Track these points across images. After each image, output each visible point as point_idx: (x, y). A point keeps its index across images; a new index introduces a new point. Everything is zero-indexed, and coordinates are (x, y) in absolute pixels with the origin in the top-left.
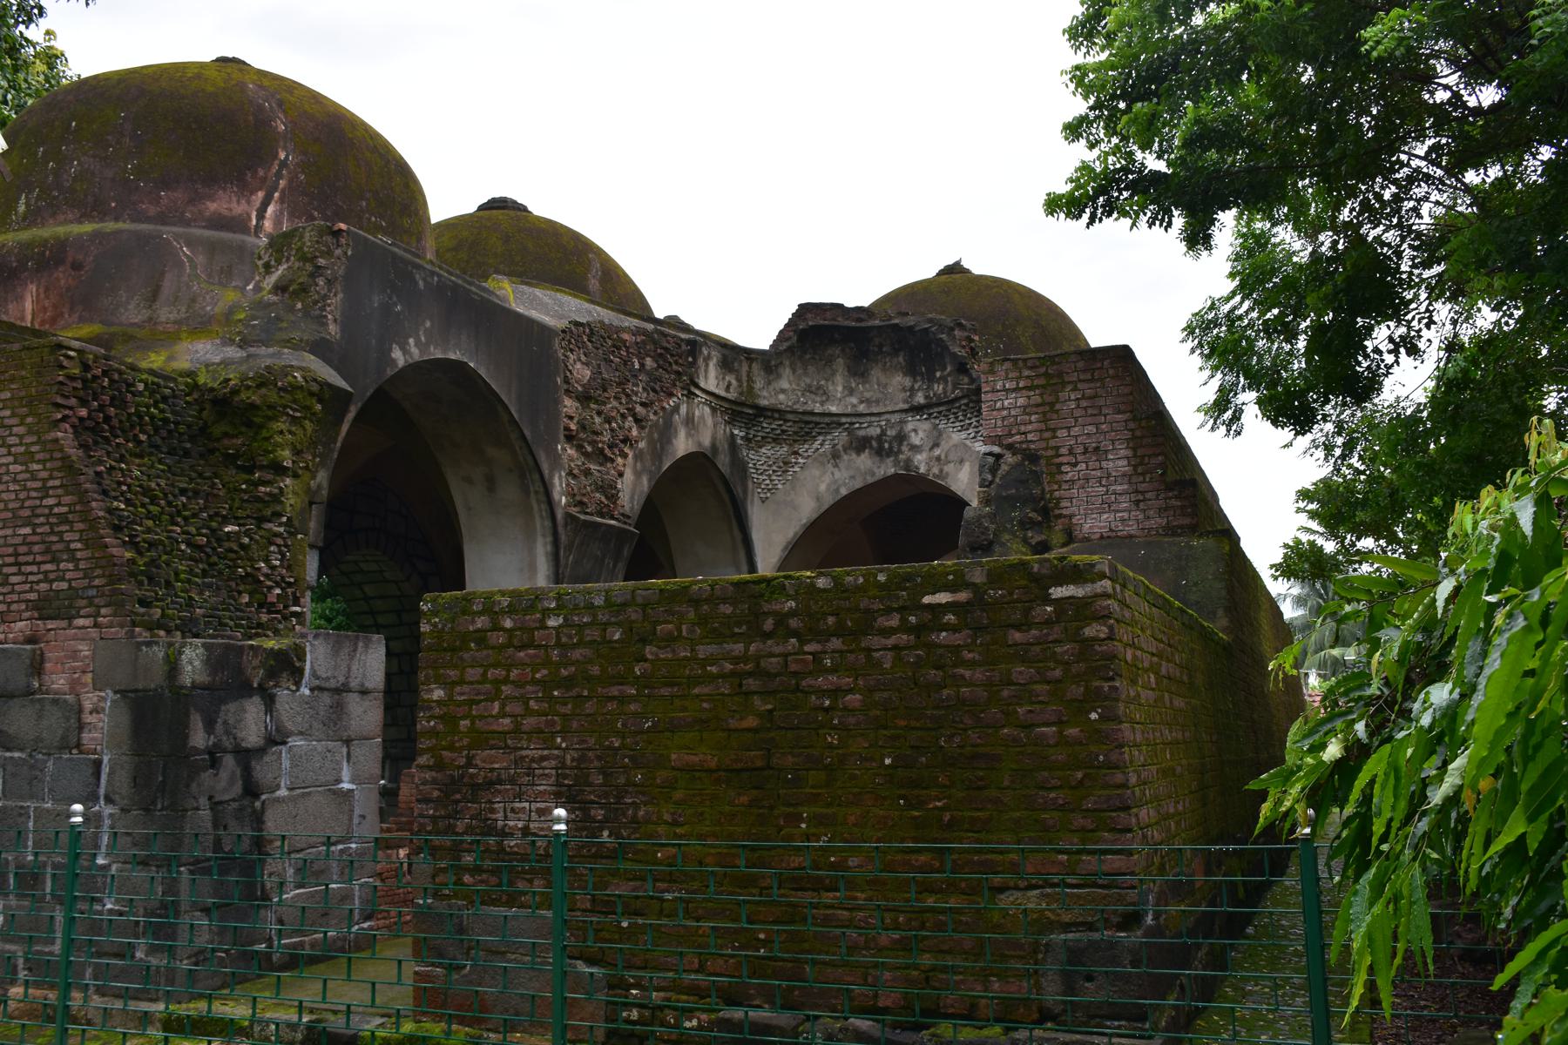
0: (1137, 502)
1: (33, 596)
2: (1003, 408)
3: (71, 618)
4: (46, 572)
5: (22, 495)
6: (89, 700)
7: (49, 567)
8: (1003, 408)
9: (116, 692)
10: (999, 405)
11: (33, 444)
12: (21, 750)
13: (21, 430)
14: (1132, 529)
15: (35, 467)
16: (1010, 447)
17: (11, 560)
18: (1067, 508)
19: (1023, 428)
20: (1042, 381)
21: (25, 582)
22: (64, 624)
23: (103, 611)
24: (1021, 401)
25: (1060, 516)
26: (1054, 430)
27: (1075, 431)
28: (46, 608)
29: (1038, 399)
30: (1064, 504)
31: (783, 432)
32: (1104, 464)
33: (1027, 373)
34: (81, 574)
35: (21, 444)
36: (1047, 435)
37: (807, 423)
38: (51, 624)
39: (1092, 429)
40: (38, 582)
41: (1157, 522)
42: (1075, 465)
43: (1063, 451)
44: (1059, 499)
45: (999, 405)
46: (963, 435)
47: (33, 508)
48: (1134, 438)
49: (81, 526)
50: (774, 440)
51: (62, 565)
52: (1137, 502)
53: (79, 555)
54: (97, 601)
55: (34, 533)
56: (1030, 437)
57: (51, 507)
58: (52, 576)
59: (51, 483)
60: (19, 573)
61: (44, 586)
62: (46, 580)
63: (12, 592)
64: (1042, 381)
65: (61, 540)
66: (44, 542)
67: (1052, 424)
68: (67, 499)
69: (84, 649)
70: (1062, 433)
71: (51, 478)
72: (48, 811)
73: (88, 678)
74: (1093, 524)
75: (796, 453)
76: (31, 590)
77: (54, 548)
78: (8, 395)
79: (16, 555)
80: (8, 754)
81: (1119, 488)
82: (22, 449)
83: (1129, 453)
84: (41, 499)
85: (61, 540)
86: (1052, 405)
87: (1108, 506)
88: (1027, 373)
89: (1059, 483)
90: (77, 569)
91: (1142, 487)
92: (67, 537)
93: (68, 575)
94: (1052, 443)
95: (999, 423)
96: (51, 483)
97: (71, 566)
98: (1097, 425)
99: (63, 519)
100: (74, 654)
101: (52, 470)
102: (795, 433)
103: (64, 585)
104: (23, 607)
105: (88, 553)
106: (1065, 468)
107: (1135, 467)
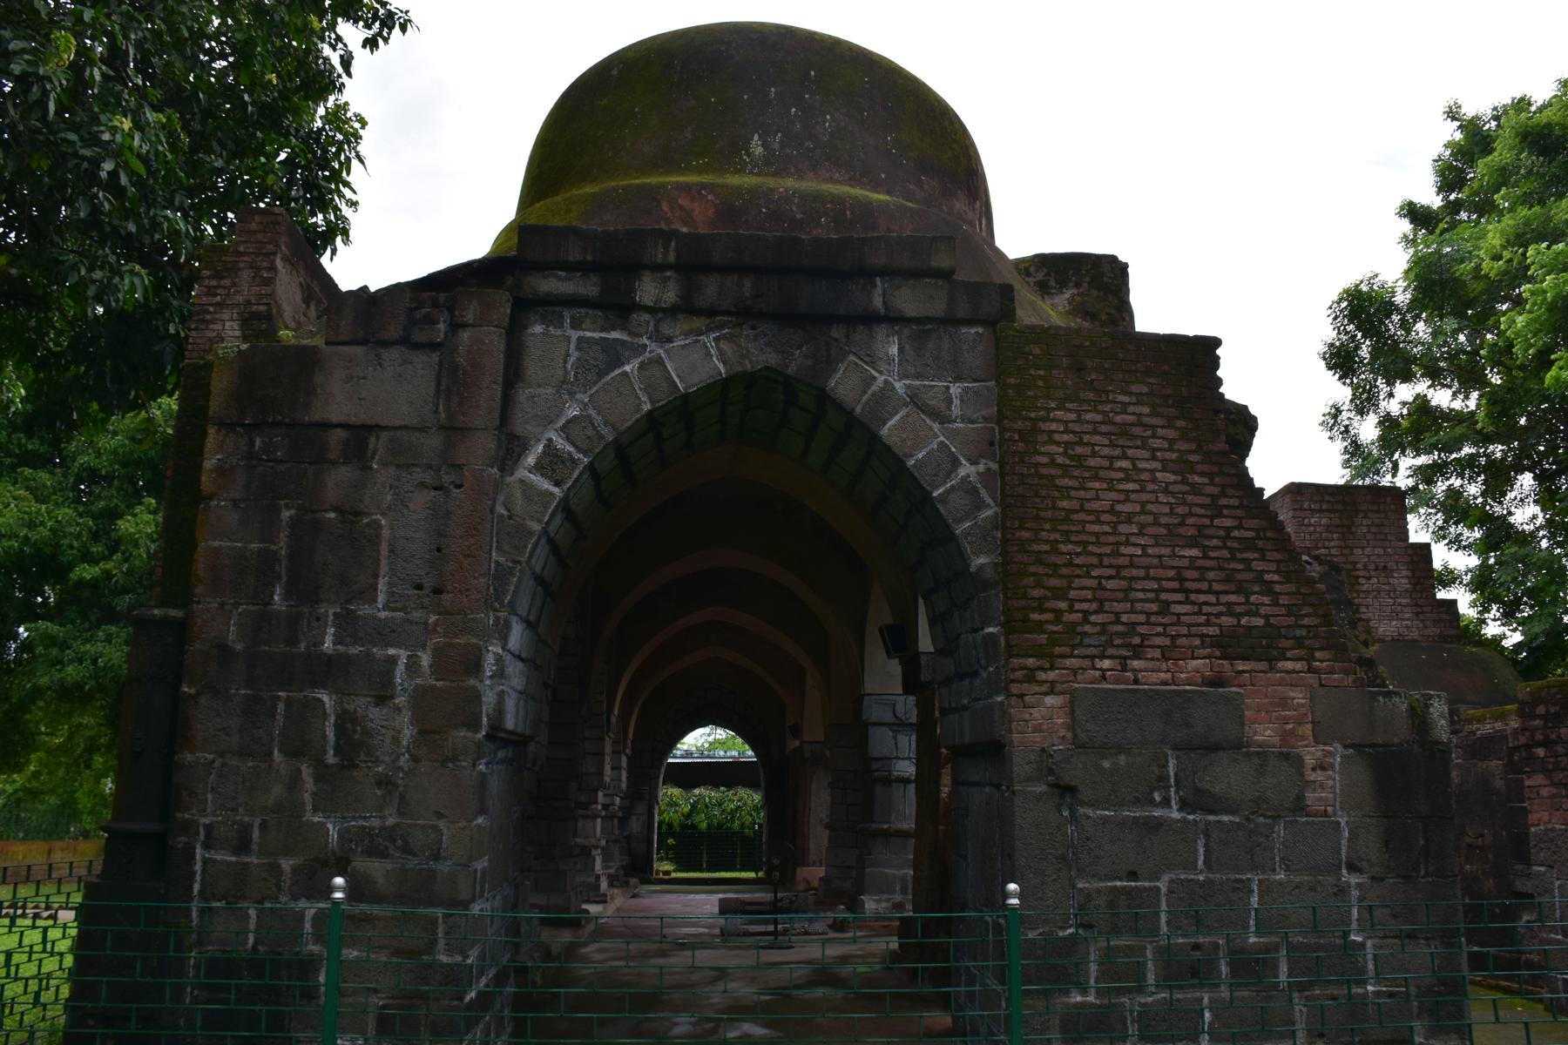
0: (1417, 614)
1: (1212, 631)
3: (1271, 661)
4: (1229, 605)
5: (1180, 510)
6: (1311, 754)
7: (1233, 598)
8: (1310, 525)
9: (1346, 747)
11: (1190, 452)
12: (1233, 813)
13: (1171, 434)
14: (1414, 635)
15: (1197, 479)
16: (1317, 558)
17: (1175, 585)
18: (1365, 613)
20: (1340, 507)
21: (1199, 613)
22: (1263, 665)
23: (1318, 654)
24: (1324, 521)
25: (1360, 619)
26: (1352, 548)
27: (1368, 551)
28: (1230, 645)
29: (1336, 521)
30: (1363, 609)
34: (1283, 611)
35: (1171, 449)
36: (1346, 551)
38: (1241, 666)
39: (1380, 551)
40: (1218, 615)
41: (1433, 631)
42: (1369, 578)
43: (1359, 566)
44: (1359, 605)
47: (1200, 528)
48: (1412, 562)
49: (1278, 556)
51: (1253, 598)
52: (1417, 614)
53: (1278, 588)
54: (1307, 642)
55: (1205, 557)
56: (1333, 551)
57: (1228, 530)
58: (1239, 609)
59: (1223, 501)
60: (1187, 601)
61: (1227, 621)
62: (1231, 614)
63: (1178, 623)
64: (1340, 507)
65: (1248, 569)
66: (1221, 569)
67: (1350, 543)
68: (1253, 523)
69: (1299, 697)
70: (1358, 552)
71: (1223, 495)
72: (1280, 883)
73: (1307, 729)
74: (1387, 628)
76: (1208, 623)
77: (1239, 577)
78: (1145, 390)
79: (1182, 580)
80: (1211, 818)
81: (1404, 601)
82: (1174, 456)
83: (1409, 574)
84: (1212, 518)
85: (1248, 569)
86: (1349, 527)
87: (1395, 615)
88: (1327, 498)
89: (1358, 592)
90: (1276, 603)
91: (1421, 602)
92: (1258, 566)
93: (1263, 610)
94: (1351, 558)
96: (1223, 501)
97: (1266, 600)
98: (1384, 548)
99: (1248, 545)
100: (1284, 703)
101: (1223, 487)
103: (1260, 622)
104: (1197, 642)
105: (1286, 588)
106: (1362, 581)
107: (1414, 585)
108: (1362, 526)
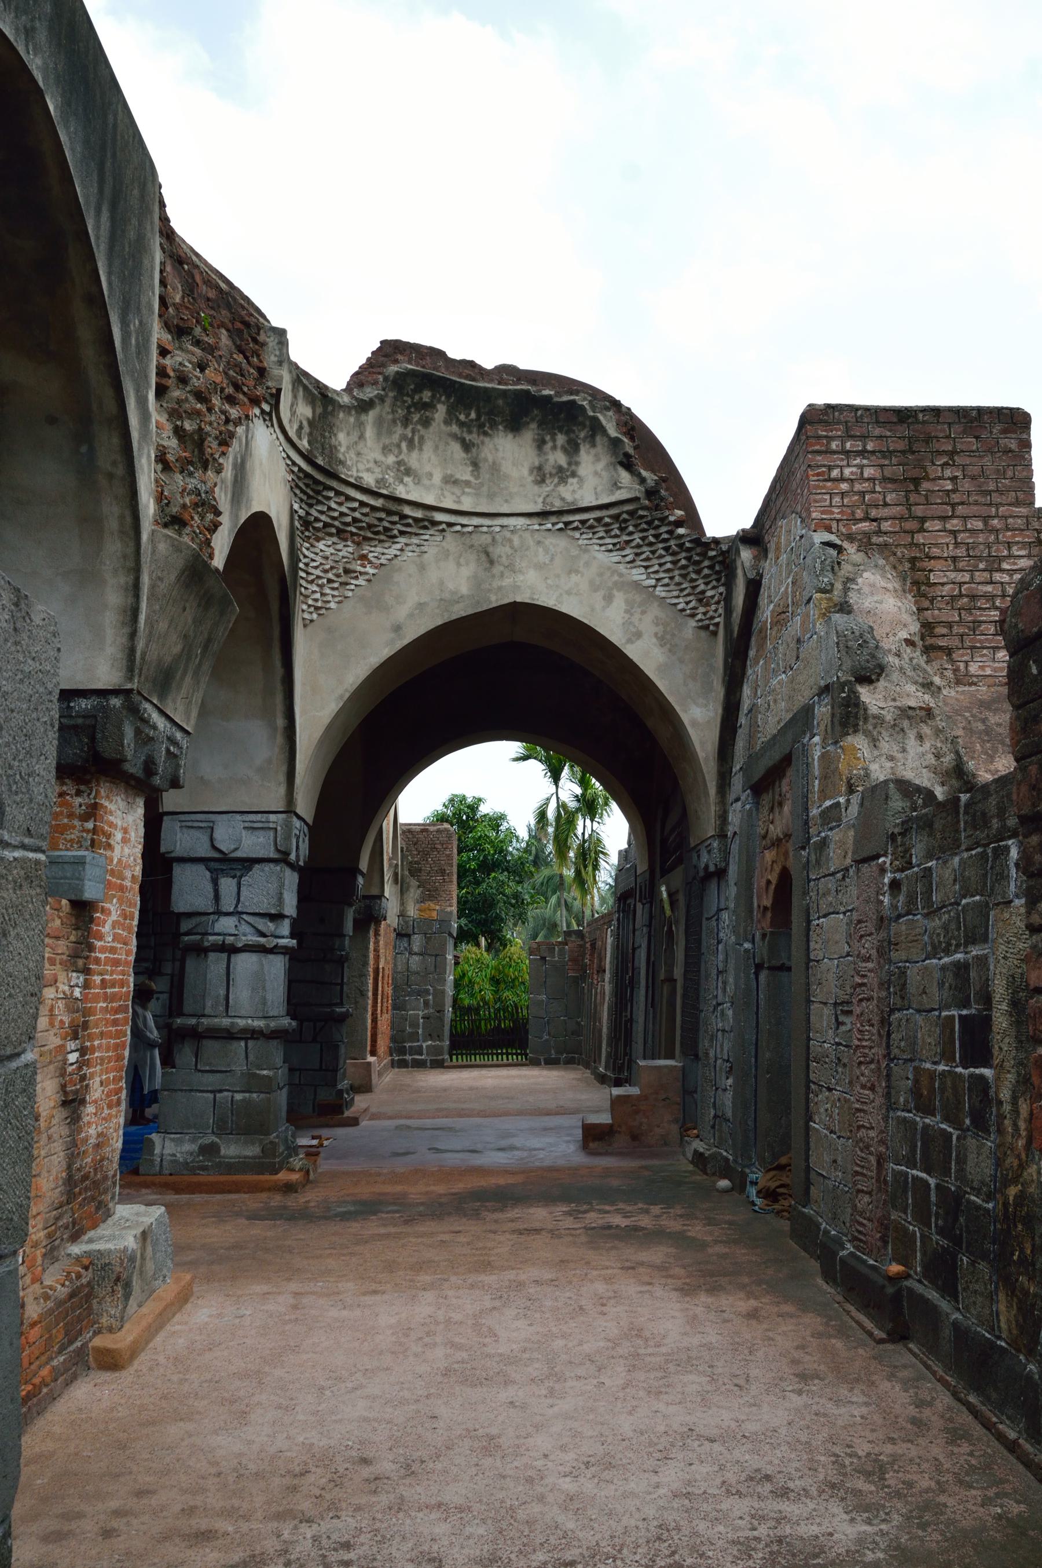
2: (842, 479)
10: (835, 473)
19: (873, 513)
24: (868, 472)
26: (923, 520)
31: (355, 520)
32: (997, 576)
33: (877, 432)
37: (390, 513)
39: (979, 525)
45: (835, 473)
46: (615, 557)
50: (340, 532)
56: (886, 526)
75: (363, 557)
86: (916, 481)
88: (877, 432)
95: (837, 500)
98: (986, 519)
102: (370, 526)
108: (942, 478)
